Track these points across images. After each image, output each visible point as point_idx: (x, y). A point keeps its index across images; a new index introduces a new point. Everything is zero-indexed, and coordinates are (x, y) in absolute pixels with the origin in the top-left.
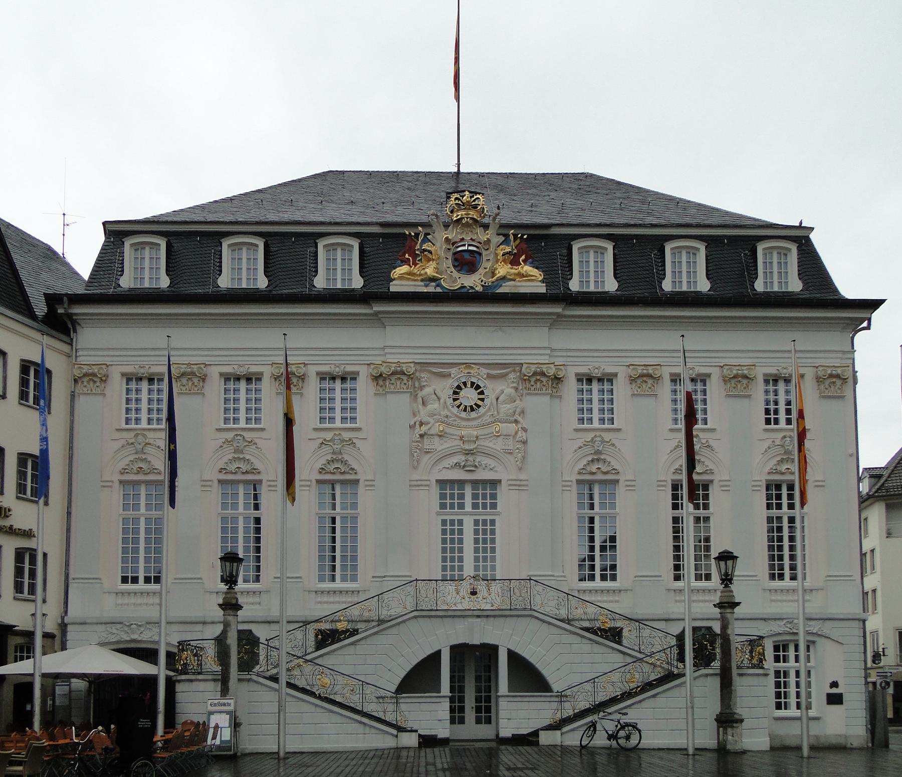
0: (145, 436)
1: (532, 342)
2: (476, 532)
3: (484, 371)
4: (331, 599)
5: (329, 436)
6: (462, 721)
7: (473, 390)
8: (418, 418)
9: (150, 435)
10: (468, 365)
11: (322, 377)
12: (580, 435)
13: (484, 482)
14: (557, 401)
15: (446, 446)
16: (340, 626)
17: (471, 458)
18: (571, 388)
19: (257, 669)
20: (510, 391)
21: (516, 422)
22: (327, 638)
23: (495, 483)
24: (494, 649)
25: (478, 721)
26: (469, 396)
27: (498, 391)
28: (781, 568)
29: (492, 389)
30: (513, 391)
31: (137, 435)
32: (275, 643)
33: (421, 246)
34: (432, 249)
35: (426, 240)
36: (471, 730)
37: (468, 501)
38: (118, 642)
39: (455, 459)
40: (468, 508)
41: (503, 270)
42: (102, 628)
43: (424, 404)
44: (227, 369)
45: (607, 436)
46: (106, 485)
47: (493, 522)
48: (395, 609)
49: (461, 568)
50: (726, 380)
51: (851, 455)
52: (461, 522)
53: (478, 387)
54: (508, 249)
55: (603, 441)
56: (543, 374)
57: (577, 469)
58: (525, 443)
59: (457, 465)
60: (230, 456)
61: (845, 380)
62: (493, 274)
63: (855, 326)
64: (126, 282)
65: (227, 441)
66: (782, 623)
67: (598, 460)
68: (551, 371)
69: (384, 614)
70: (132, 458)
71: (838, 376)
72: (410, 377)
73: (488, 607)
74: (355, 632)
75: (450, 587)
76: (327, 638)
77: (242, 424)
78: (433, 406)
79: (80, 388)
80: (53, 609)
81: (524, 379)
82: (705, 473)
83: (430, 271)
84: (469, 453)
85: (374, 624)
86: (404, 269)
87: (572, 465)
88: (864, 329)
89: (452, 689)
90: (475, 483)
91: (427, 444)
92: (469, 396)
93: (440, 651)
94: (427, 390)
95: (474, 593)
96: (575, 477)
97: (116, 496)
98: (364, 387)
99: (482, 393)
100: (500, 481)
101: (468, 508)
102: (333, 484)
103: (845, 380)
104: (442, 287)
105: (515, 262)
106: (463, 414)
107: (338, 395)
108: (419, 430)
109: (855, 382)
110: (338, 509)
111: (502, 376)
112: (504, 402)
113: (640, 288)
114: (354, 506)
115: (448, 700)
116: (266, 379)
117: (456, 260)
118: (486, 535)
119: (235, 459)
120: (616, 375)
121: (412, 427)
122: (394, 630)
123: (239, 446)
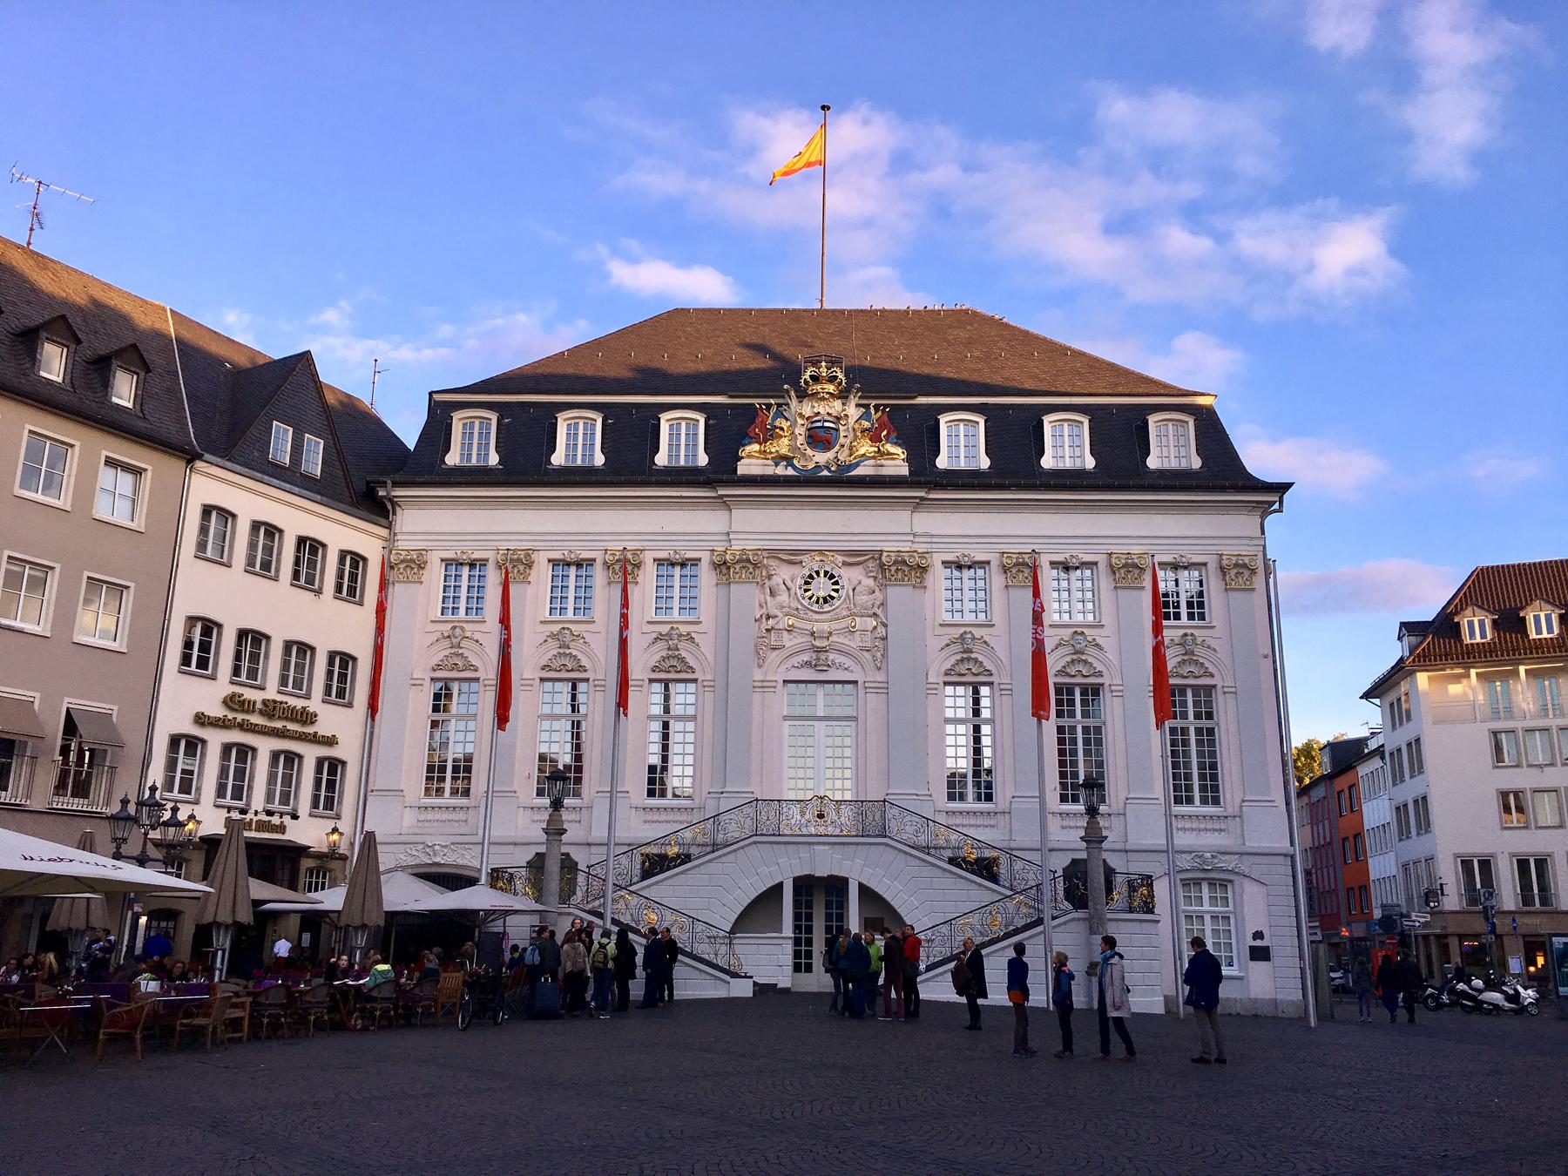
0: (462, 629)
3: (840, 559)
5: (665, 629)
8: (764, 611)
11: (659, 562)
12: (947, 630)
14: (919, 592)
15: (796, 641)
16: (672, 851)
17: (823, 656)
18: (938, 577)
22: (656, 865)
24: (845, 881)
26: (822, 587)
28: (1189, 788)
30: (871, 582)
31: (454, 628)
32: (598, 870)
33: (774, 419)
34: (785, 425)
35: (779, 414)
39: (806, 657)
41: (866, 448)
48: (733, 831)
50: (1113, 570)
51: (1266, 657)
53: (832, 577)
54: (866, 424)
55: (974, 638)
56: (904, 562)
57: (943, 670)
58: (884, 639)
59: (808, 664)
60: (555, 652)
61: (1253, 572)
63: (1265, 510)
64: (453, 459)
65: (552, 636)
66: (1189, 857)
67: (969, 659)
69: (720, 838)
70: (447, 652)
71: (1245, 566)
73: (837, 832)
74: (686, 858)
76: (656, 865)
77: (570, 614)
78: (783, 597)
80: (345, 825)
81: (882, 565)
82: (1093, 675)
83: (782, 446)
84: (818, 650)
85: (709, 849)
86: (756, 447)
88: (1275, 511)
89: (797, 928)
91: (773, 639)
92: (822, 587)
93: (780, 886)
94: (777, 580)
95: (821, 816)
100: (856, 682)
103: (1253, 572)
104: (795, 468)
105: (875, 439)
106: (815, 607)
107: (677, 583)
108: (765, 625)
113: (1015, 466)
115: (791, 942)
117: (810, 436)
120: (988, 563)
123: (562, 639)
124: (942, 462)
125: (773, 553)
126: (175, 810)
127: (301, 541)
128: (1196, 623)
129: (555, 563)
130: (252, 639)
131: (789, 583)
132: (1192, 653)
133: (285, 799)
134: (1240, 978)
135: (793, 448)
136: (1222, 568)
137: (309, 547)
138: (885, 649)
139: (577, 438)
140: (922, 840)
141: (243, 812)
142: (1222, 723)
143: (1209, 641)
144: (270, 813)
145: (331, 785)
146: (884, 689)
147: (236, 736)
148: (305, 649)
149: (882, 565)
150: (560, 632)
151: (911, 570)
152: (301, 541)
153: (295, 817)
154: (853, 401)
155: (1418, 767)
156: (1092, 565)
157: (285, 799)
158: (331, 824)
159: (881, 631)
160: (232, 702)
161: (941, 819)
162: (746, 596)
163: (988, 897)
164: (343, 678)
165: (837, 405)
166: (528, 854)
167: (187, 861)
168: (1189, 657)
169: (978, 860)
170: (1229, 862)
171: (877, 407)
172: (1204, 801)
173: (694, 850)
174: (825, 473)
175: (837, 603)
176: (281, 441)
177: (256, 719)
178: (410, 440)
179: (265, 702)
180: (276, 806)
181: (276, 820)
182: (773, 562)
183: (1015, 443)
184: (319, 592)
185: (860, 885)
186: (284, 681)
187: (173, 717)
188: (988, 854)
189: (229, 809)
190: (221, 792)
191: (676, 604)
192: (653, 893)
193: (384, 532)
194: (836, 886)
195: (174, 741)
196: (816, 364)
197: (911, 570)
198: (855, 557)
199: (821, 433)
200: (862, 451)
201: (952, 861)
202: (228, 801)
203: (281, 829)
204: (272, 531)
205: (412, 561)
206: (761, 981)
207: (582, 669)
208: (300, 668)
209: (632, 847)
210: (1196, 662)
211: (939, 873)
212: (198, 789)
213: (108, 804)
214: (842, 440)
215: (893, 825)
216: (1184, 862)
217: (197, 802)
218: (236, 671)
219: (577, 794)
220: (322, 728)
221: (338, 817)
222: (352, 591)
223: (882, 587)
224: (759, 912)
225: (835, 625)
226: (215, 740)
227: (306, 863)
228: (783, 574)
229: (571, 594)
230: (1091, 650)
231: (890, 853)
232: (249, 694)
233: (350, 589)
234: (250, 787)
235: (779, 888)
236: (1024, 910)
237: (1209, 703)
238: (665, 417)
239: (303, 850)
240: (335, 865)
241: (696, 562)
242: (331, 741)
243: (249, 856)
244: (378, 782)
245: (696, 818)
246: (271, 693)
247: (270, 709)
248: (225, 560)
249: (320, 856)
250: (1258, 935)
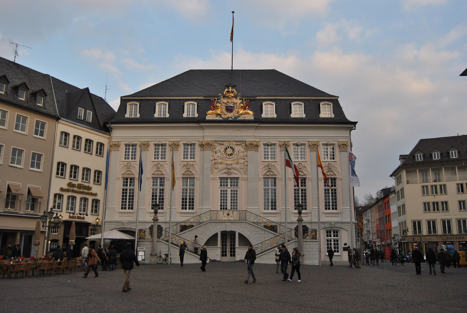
1: (249, 135)
2: (231, 194)
3: (234, 143)
4: (186, 215)
5: (186, 163)
6: (226, 255)
7: (231, 149)
9: (131, 163)
10: (229, 141)
11: (184, 144)
13: (234, 178)
14: (257, 152)
15: (222, 166)
16: (188, 224)
18: (262, 148)
19: (162, 237)
20: (242, 149)
21: (244, 159)
22: (184, 228)
23: (237, 178)
25: (231, 255)
26: (229, 151)
27: (238, 149)
29: (237, 148)
30: (243, 149)
35: (218, 102)
36: (228, 258)
37: (229, 184)
38: (120, 228)
40: (229, 186)
41: (241, 111)
42: (115, 223)
43: (216, 153)
44: (156, 143)
45: (272, 164)
46: (118, 179)
47: (237, 191)
49: (226, 206)
50: (310, 146)
52: (227, 191)
54: (242, 105)
56: (252, 144)
58: (247, 166)
59: (226, 173)
62: (238, 112)
63: (351, 129)
64: (127, 116)
66: (328, 224)
67: (270, 171)
68: (255, 144)
69: (201, 221)
70: (126, 170)
71: (345, 145)
72: (211, 145)
73: (233, 219)
74: (193, 226)
75: (221, 213)
76: (184, 228)
78: (219, 154)
79: (112, 149)
80: (100, 217)
82: (304, 175)
84: (229, 169)
87: (262, 172)
89: (222, 245)
90: (231, 178)
92: (229, 151)
93: (217, 233)
94: (217, 149)
95: (228, 215)
96: (262, 177)
97: (121, 182)
98: (197, 149)
99: (234, 150)
101: (229, 186)
102: (187, 178)
104: (222, 117)
105: (245, 109)
106: (228, 157)
107: (189, 150)
109: (351, 146)
110: (188, 186)
111: (240, 144)
112: (240, 153)
114: (193, 185)
116: (167, 146)
118: (235, 195)
119: (157, 171)
120: (276, 144)
121: (212, 161)
122: (204, 226)
123: (158, 167)
124: (263, 116)
125: (216, 141)
126: (57, 214)
127: (87, 140)
128: (332, 160)
129: (155, 145)
130: (75, 168)
131: (221, 150)
132: (330, 169)
133: (84, 210)
134: (340, 256)
135: (221, 112)
136: (339, 145)
137: (89, 142)
138: (247, 168)
139: (161, 110)
140: (256, 221)
141: (74, 214)
142: (338, 188)
143: (335, 166)
144: (80, 214)
145: (96, 207)
146: (246, 179)
147: (71, 194)
148: (88, 170)
149: (246, 145)
150: (157, 164)
151: (254, 146)
152: (87, 140)
153: (87, 215)
154: (238, 98)
155: (403, 196)
156: (304, 144)
157: (84, 210)
158: (96, 217)
159: (246, 163)
160: (70, 185)
161: (262, 215)
162: (208, 153)
163: (273, 236)
164: (98, 177)
166: (150, 225)
167: (60, 227)
168: (330, 170)
169: (271, 226)
170: (338, 225)
171: (245, 100)
172: (333, 209)
173: (194, 224)
174: (231, 119)
175: (233, 155)
176: (81, 112)
177: (76, 189)
178: (116, 109)
179: (78, 184)
180: (82, 212)
181: (82, 216)
182: (216, 144)
183: (284, 109)
184: (91, 154)
185: (239, 233)
186: (83, 179)
187: (55, 189)
188: (275, 224)
189: (70, 213)
190: (68, 209)
191: (189, 156)
192: (183, 236)
193: (108, 137)
194: (232, 234)
195: (55, 195)
196: (228, 88)
197: (254, 146)
198: (239, 143)
199: (230, 107)
200: (241, 112)
201: (265, 227)
202: (69, 211)
203: (84, 218)
204: (79, 138)
205: (116, 145)
206: (212, 259)
207: (163, 174)
208: (87, 175)
209: (177, 223)
210: (332, 171)
211: (260, 230)
212: (62, 208)
213: (39, 212)
214: (235, 110)
215: (248, 217)
216: (327, 225)
217: (61, 211)
218: (71, 176)
219: (162, 209)
220: (93, 191)
221: (98, 215)
222: (100, 153)
223: (246, 151)
224: (212, 240)
225: (233, 162)
226: (66, 195)
227: (90, 228)
228: (218, 148)
229: (160, 154)
230: (304, 168)
231: (247, 225)
232: (74, 182)
233: (100, 152)
234: (75, 207)
235: (217, 234)
236: (281, 239)
237: (335, 183)
238: (186, 104)
239: (89, 224)
240: (97, 228)
241: (194, 144)
242: (96, 195)
243: (76, 225)
244: (109, 206)
245: (195, 215)
246: (80, 182)
247: (80, 186)
248: (67, 146)
249: (94, 225)
250: (346, 244)
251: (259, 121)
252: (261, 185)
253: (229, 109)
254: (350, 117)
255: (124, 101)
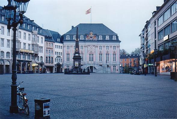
41: (94, 38)
50: (110, 47)
83: (88, 38)
87: (99, 53)
113: (104, 40)
162: (86, 48)
165: (92, 35)
183: (104, 37)
198: (94, 46)
251: (98, 41)
252: (98, 55)
253: (91, 38)
254: (120, 40)
255: (65, 35)
